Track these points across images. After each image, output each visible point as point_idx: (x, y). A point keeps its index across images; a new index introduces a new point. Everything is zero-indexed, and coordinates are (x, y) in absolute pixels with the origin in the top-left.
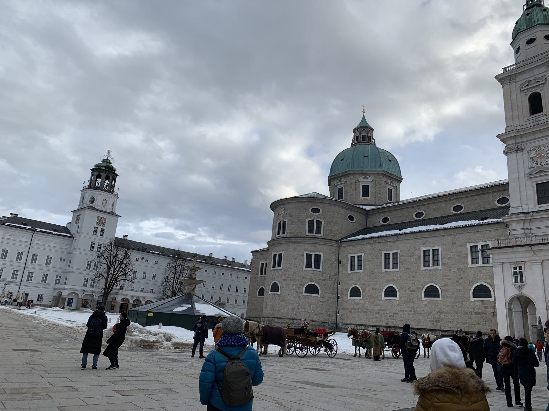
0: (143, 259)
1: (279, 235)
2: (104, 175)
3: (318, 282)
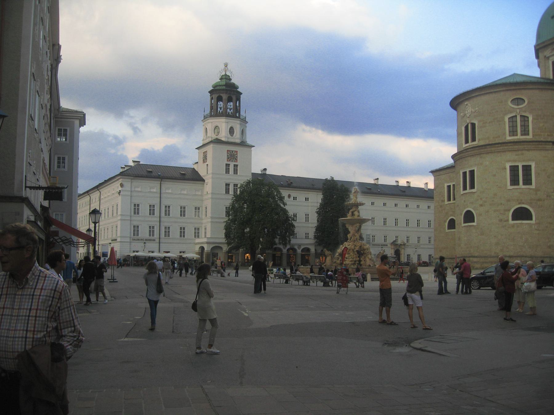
0: (289, 196)
1: (467, 145)
2: (225, 97)
3: (530, 204)
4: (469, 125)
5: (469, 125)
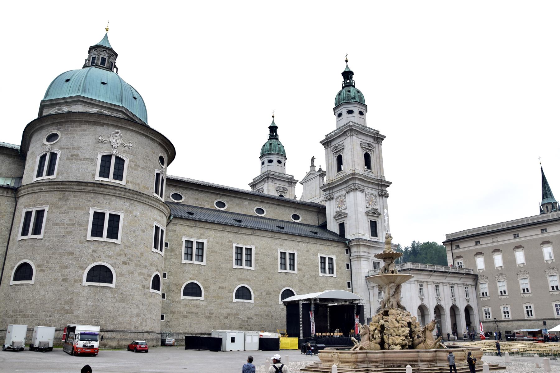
4: (113, 159)
5: (113, 159)
